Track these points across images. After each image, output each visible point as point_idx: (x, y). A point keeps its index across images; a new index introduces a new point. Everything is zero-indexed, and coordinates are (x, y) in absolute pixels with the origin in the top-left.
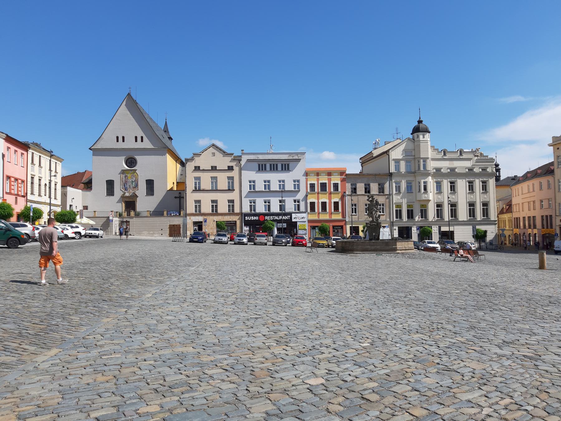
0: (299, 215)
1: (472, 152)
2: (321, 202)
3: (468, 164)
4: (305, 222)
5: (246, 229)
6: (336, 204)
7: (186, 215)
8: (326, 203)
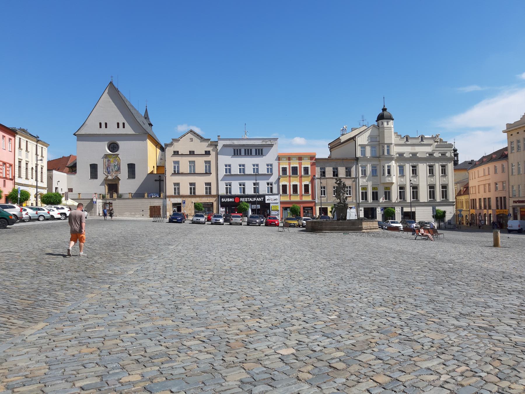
0: (272, 197)
1: (432, 138)
2: (304, 185)
3: (429, 149)
4: (277, 203)
5: (222, 210)
6: (306, 186)
7: (166, 197)
8: (296, 185)
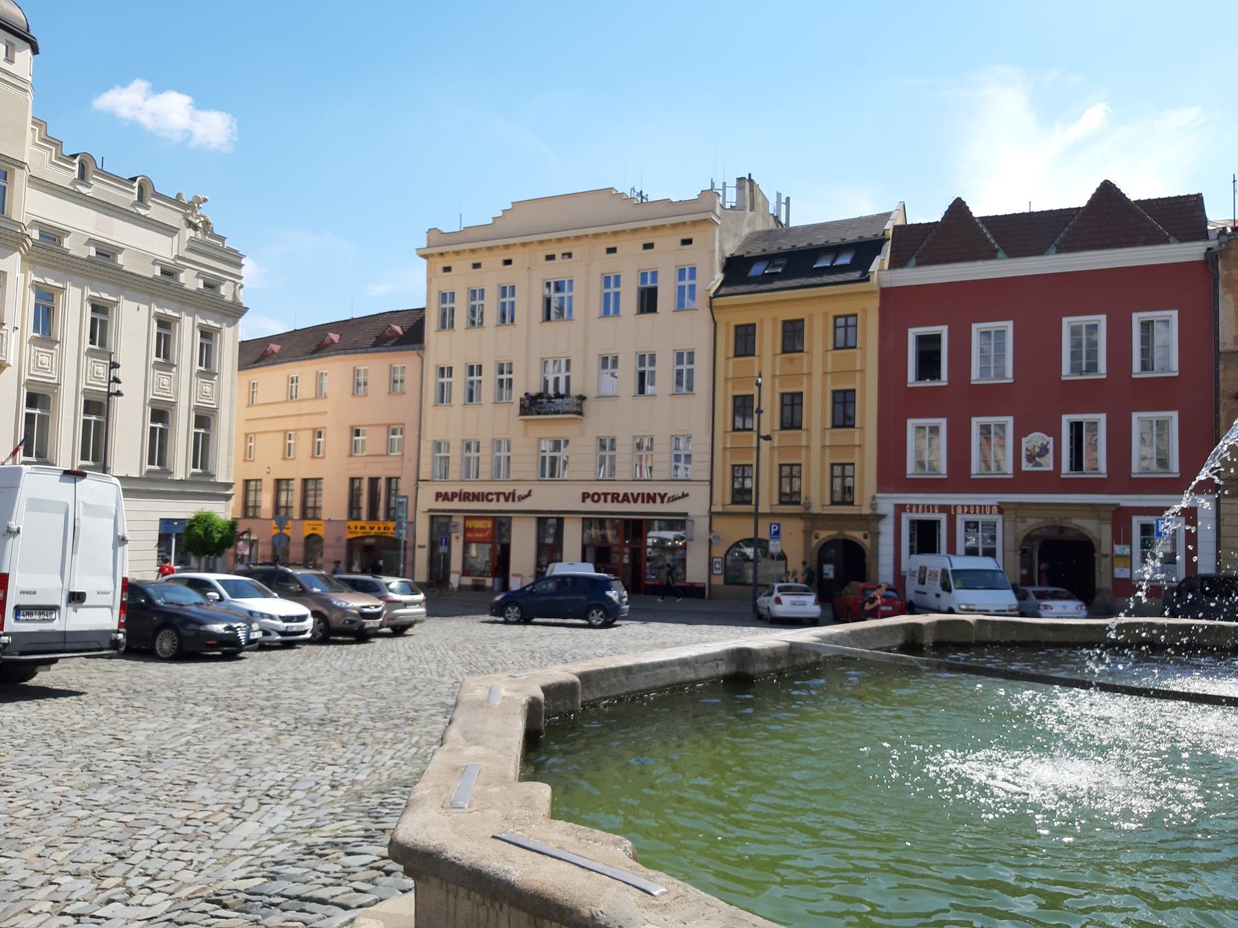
3: (164, 248)
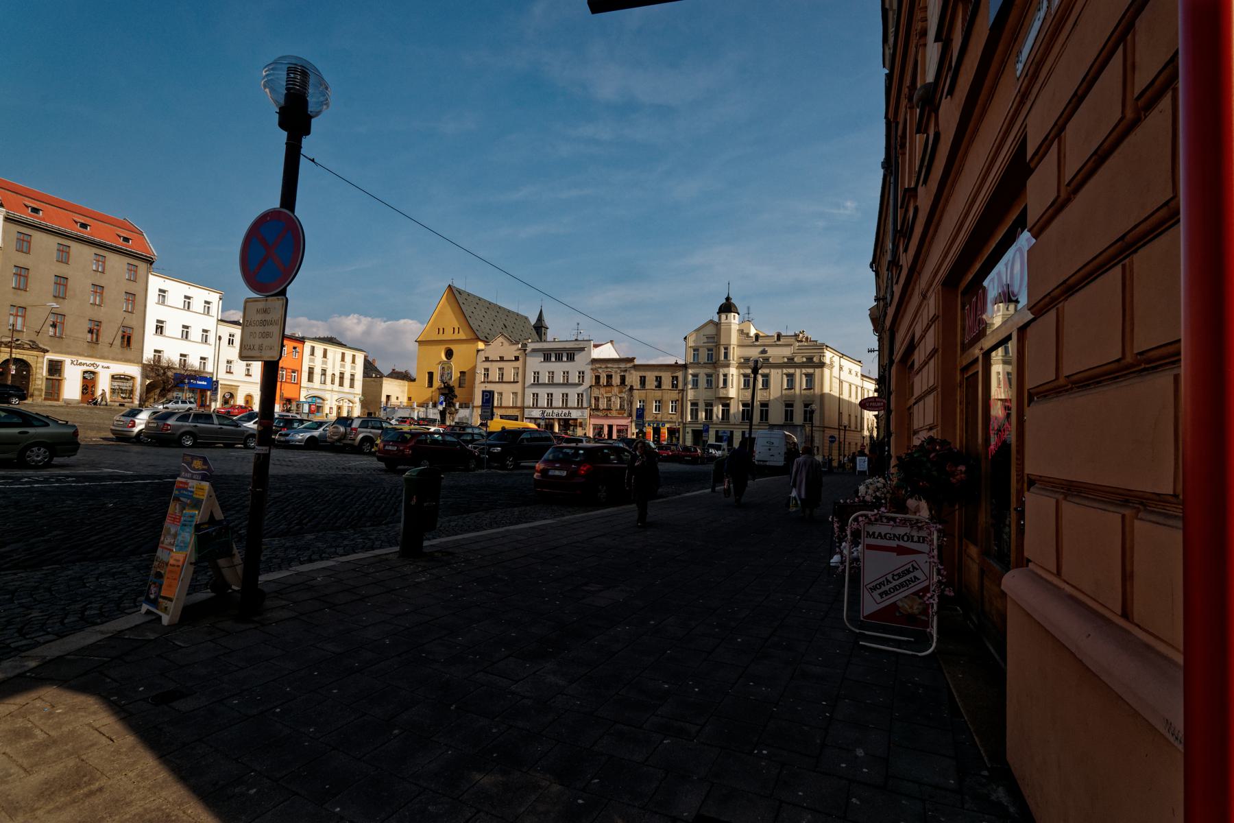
1: (796, 336)
3: (787, 352)
7: (473, 407)
